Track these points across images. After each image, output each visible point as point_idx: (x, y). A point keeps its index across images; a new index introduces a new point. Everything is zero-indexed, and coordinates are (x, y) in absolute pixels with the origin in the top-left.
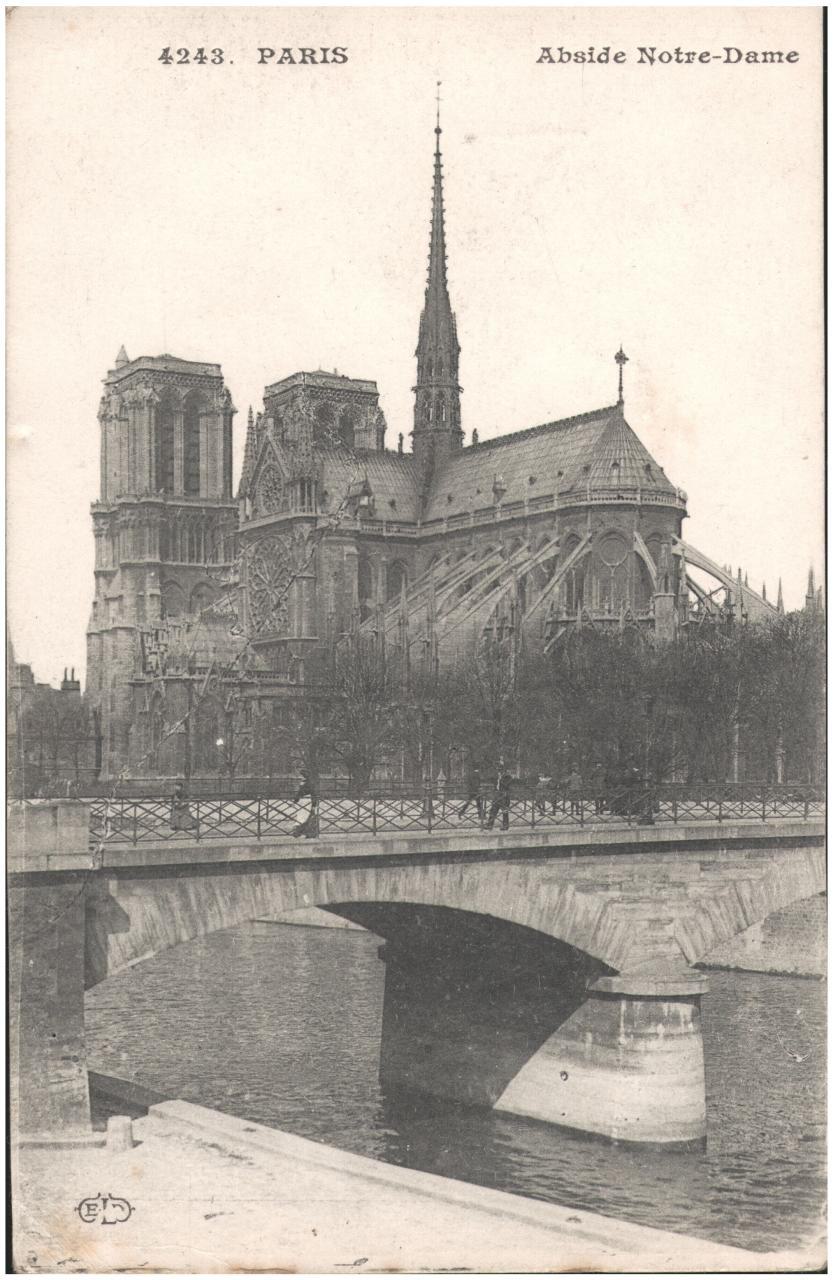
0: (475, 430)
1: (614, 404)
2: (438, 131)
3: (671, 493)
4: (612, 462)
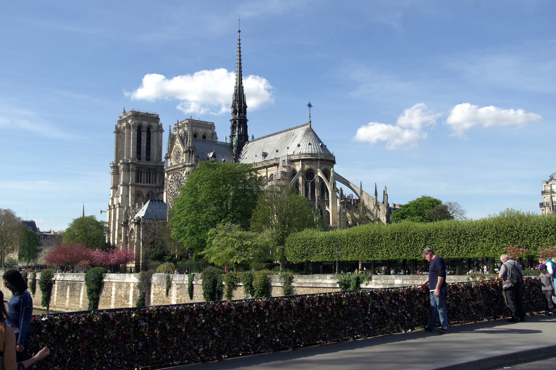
0: (253, 135)
1: (307, 123)
2: (239, 32)
3: (331, 155)
4: (308, 143)
